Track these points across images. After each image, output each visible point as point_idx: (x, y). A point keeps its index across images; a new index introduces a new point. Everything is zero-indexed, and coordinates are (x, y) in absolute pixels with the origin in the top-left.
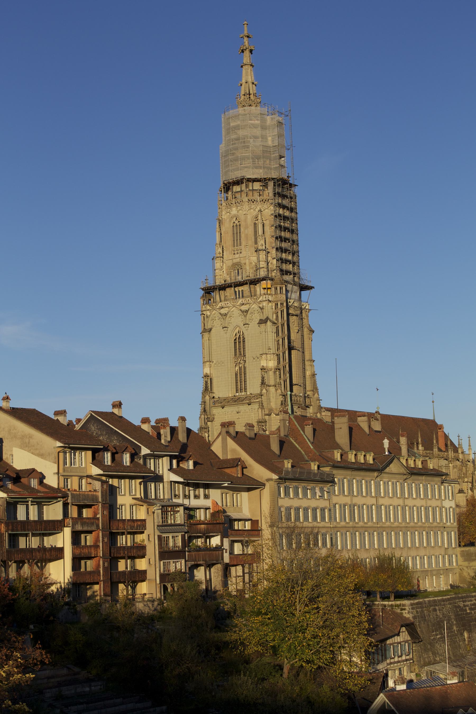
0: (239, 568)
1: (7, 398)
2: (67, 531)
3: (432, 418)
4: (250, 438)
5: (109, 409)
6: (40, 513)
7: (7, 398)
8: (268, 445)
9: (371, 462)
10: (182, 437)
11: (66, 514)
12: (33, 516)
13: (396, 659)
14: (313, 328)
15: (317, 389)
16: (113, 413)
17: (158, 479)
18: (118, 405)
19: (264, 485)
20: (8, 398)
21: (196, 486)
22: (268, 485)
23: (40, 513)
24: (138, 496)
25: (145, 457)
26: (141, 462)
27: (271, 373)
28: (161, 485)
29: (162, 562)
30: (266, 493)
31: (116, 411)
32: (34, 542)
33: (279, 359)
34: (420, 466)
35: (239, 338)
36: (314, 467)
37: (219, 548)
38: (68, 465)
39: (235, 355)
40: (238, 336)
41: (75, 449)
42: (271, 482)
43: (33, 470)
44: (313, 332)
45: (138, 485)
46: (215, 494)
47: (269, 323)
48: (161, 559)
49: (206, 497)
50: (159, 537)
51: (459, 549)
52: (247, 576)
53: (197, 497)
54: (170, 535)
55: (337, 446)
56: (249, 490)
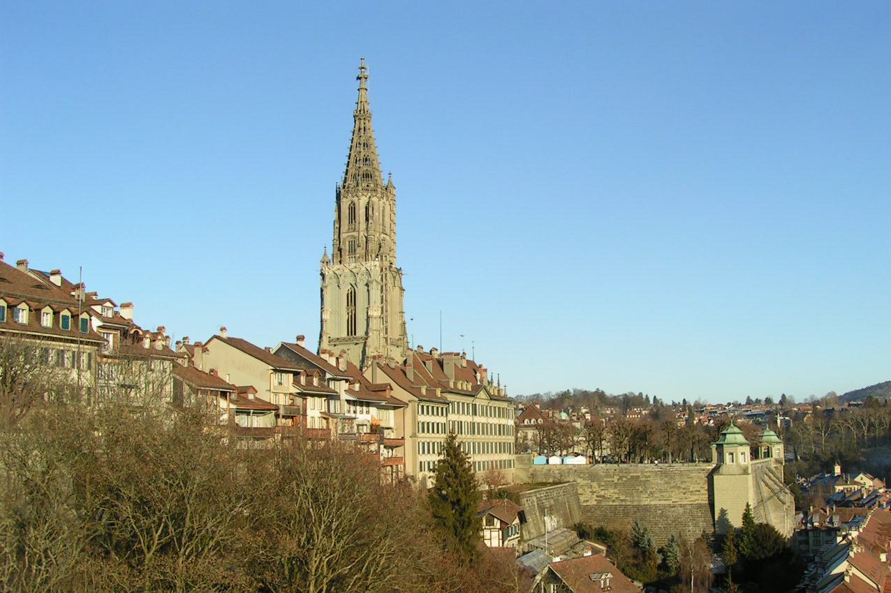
3: (472, 360)
5: (294, 341)
9: (470, 390)
13: (513, 537)
14: (404, 288)
15: (406, 334)
16: (297, 345)
18: (300, 338)
19: (408, 405)
20: (225, 329)
21: (361, 404)
22: (410, 404)
24: (323, 411)
25: (329, 379)
26: (326, 383)
28: (339, 402)
30: (409, 410)
31: (299, 343)
33: (382, 310)
34: (496, 394)
35: (351, 293)
36: (439, 394)
39: (348, 305)
40: (350, 291)
42: (413, 403)
43: (252, 387)
44: (404, 290)
45: (323, 402)
46: (373, 410)
49: (368, 412)
52: (394, 474)
53: (362, 412)
56: (395, 408)
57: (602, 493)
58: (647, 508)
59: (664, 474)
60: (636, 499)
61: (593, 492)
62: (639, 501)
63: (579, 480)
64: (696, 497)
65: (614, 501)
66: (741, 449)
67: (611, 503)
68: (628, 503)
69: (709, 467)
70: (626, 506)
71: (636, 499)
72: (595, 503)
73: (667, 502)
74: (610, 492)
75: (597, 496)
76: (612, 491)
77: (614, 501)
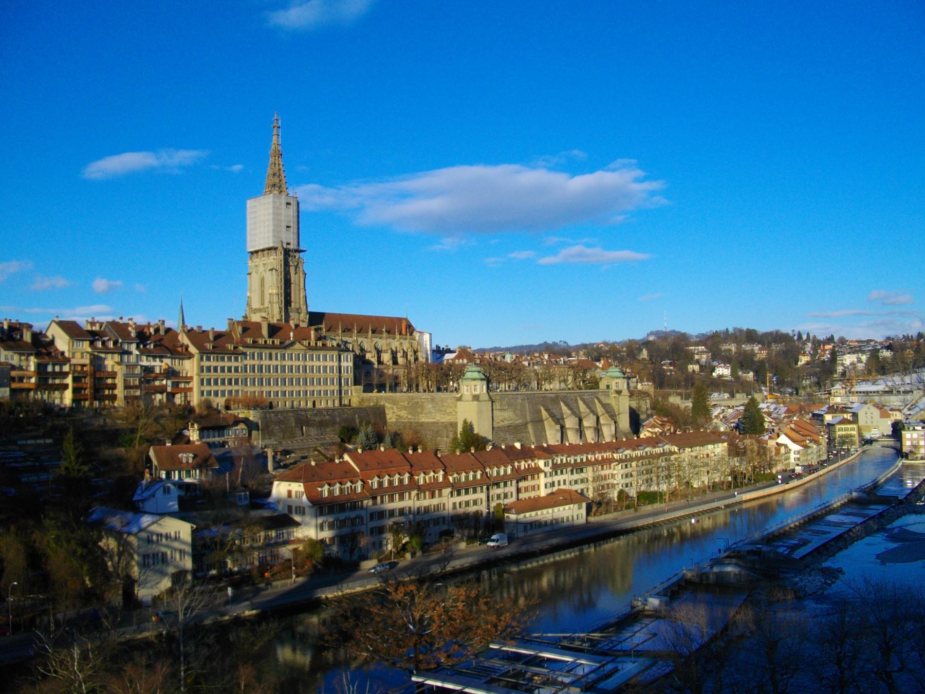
0: (179, 394)
1: (57, 317)
2: (70, 377)
3: (406, 317)
4: (199, 333)
6: (61, 368)
7: (57, 317)
8: (208, 335)
10: (162, 332)
11: (70, 369)
12: (57, 369)
17: (129, 353)
23: (61, 368)
27: (275, 296)
29: (126, 391)
32: (57, 381)
37: (166, 385)
38: (75, 347)
41: (80, 340)
46: (168, 361)
47: (274, 270)
48: (124, 389)
50: (125, 380)
51: (353, 387)
54: (132, 379)
55: (262, 336)
57: (399, 413)
58: (422, 424)
59: (433, 400)
60: (417, 417)
61: (394, 413)
62: (419, 419)
63: (387, 405)
64: (450, 417)
65: (405, 419)
66: (474, 383)
67: (403, 421)
68: (413, 421)
69: (458, 396)
70: (411, 423)
71: (417, 417)
72: (394, 420)
73: (433, 420)
74: (404, 413)
75: (396, 416)
76: (403, 412)
77: (405, 419)
